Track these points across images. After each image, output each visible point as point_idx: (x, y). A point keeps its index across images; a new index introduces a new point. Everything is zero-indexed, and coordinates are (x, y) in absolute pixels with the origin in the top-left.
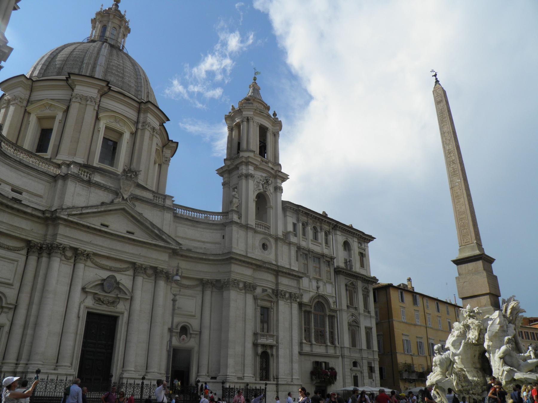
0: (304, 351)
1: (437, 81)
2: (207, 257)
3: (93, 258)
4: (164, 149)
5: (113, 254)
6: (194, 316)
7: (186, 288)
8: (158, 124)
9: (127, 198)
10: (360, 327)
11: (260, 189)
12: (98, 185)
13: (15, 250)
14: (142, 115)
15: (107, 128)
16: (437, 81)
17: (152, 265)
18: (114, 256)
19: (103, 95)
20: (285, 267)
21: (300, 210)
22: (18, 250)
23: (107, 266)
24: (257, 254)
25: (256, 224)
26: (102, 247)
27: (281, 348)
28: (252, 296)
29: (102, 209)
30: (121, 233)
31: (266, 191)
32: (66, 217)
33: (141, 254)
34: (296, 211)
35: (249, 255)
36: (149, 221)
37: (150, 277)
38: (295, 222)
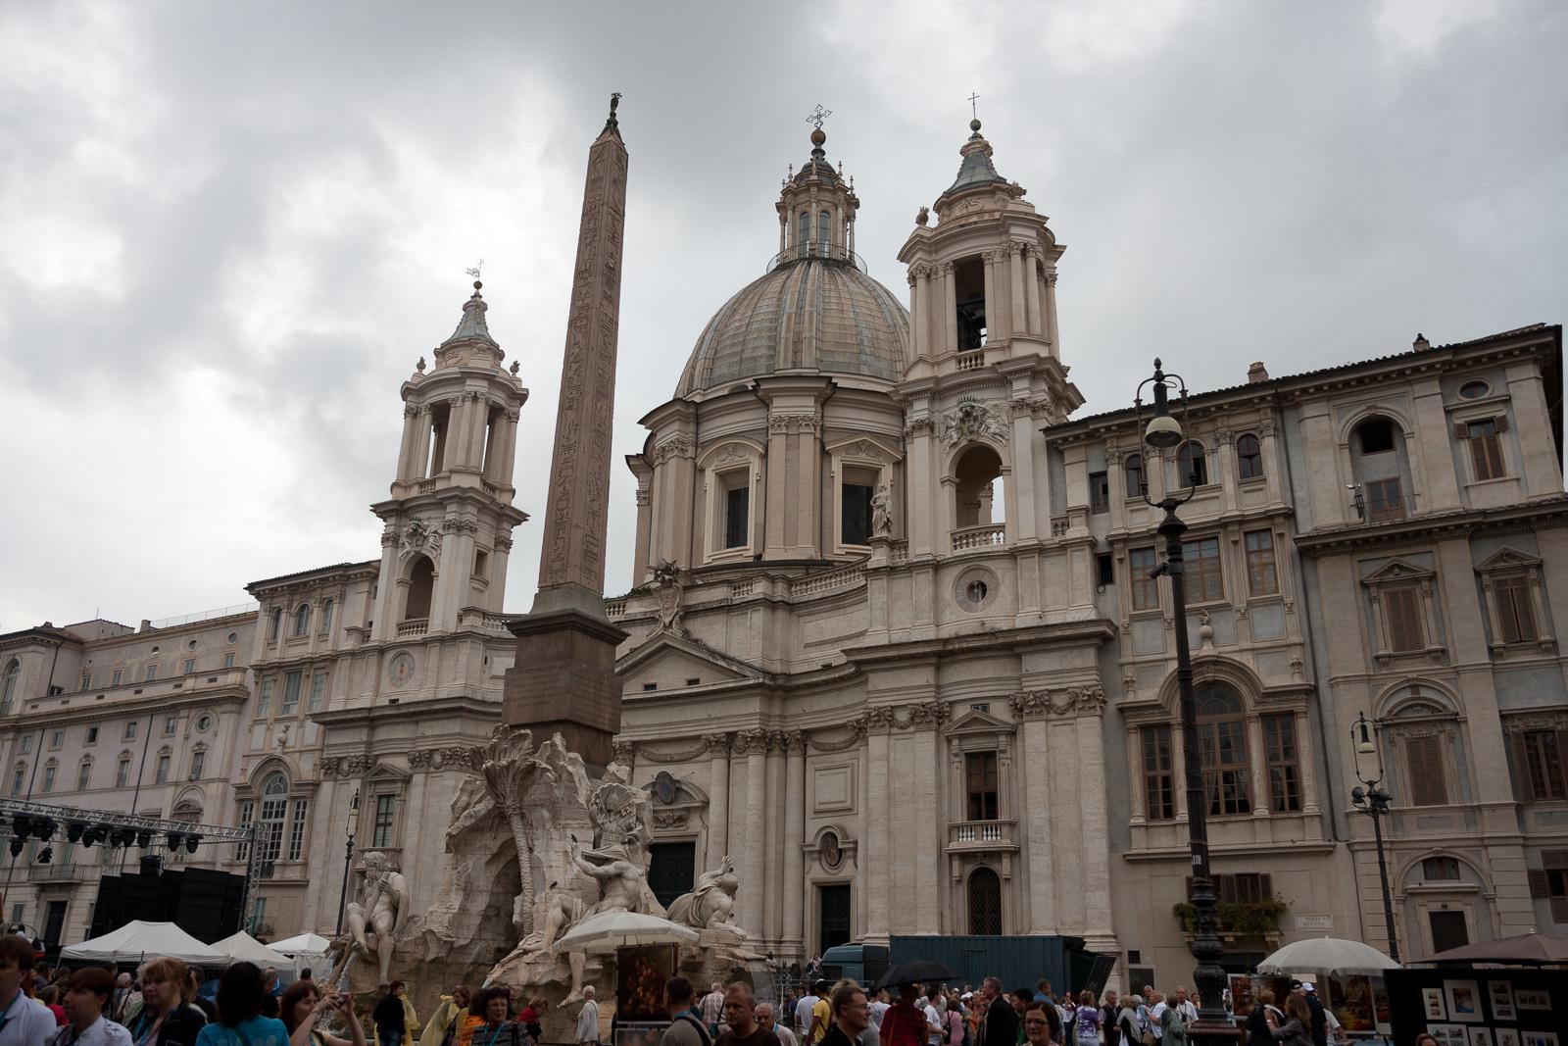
0: (1133, 852)
1: (612, 124)
2: (842, 673)
5: (667, 733)
8: (811, 401)
9: (671, 622)
10: (1466, 722)
11: (955, 444)
16: (612, 124)
17: (725, 730)
18: (669, 736)
19: (698, 420)
20: (1016, 630)
21: (1097, 430)
23: (666, 755)
24: (959, 620)
25: (955, 541)
26: (648, 726)
27: (1039, 855)
28: (933, 733)
29: (630, 663)
31: (971, 441)
34: (1090, 435)
35: (916, 636)
38: (1096, 468)
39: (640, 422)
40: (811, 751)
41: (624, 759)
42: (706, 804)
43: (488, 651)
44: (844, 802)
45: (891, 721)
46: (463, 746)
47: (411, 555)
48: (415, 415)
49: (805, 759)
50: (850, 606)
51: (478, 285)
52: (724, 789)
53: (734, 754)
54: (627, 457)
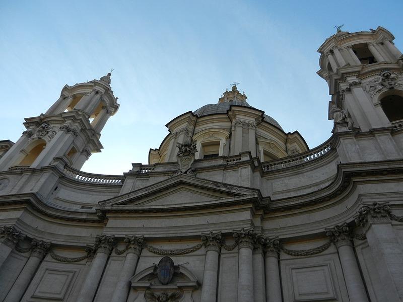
3: (151, 245)
4: (288, 145)
5: (172, 233)
6: (335, 299)
7: (306, 255)
9: (186, 172)
11: (380, 90)
12: (159, 174)
13: (75, 262)
14: (234, 121)
15: (204, 145)
22: (77, 261)
23: (167, 250)
30: (176, 204)
32: (109, 208)
33: (210, 222)
36: (212, 181)
37: (231, 250)
39: (167, 126)
40: (284, 256)
41: (135, 249)
42: (199, 286)
43: (60, 185)
44: (327, 293)
45: (392, 217)
46: (16, 228)
47: (35, 140)
48: (65, 98)
49: (279, 262)
50: (306, 172)
51: (109, 74)
52: (216, 274)
53: (223, 251)
54: (151, 150)
